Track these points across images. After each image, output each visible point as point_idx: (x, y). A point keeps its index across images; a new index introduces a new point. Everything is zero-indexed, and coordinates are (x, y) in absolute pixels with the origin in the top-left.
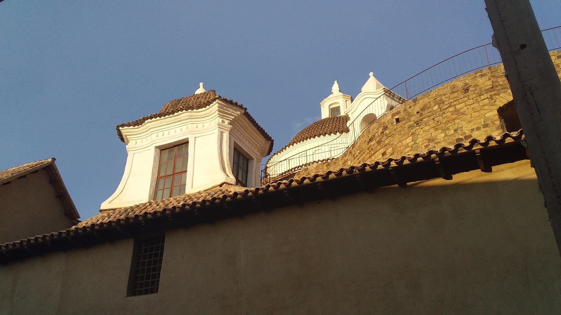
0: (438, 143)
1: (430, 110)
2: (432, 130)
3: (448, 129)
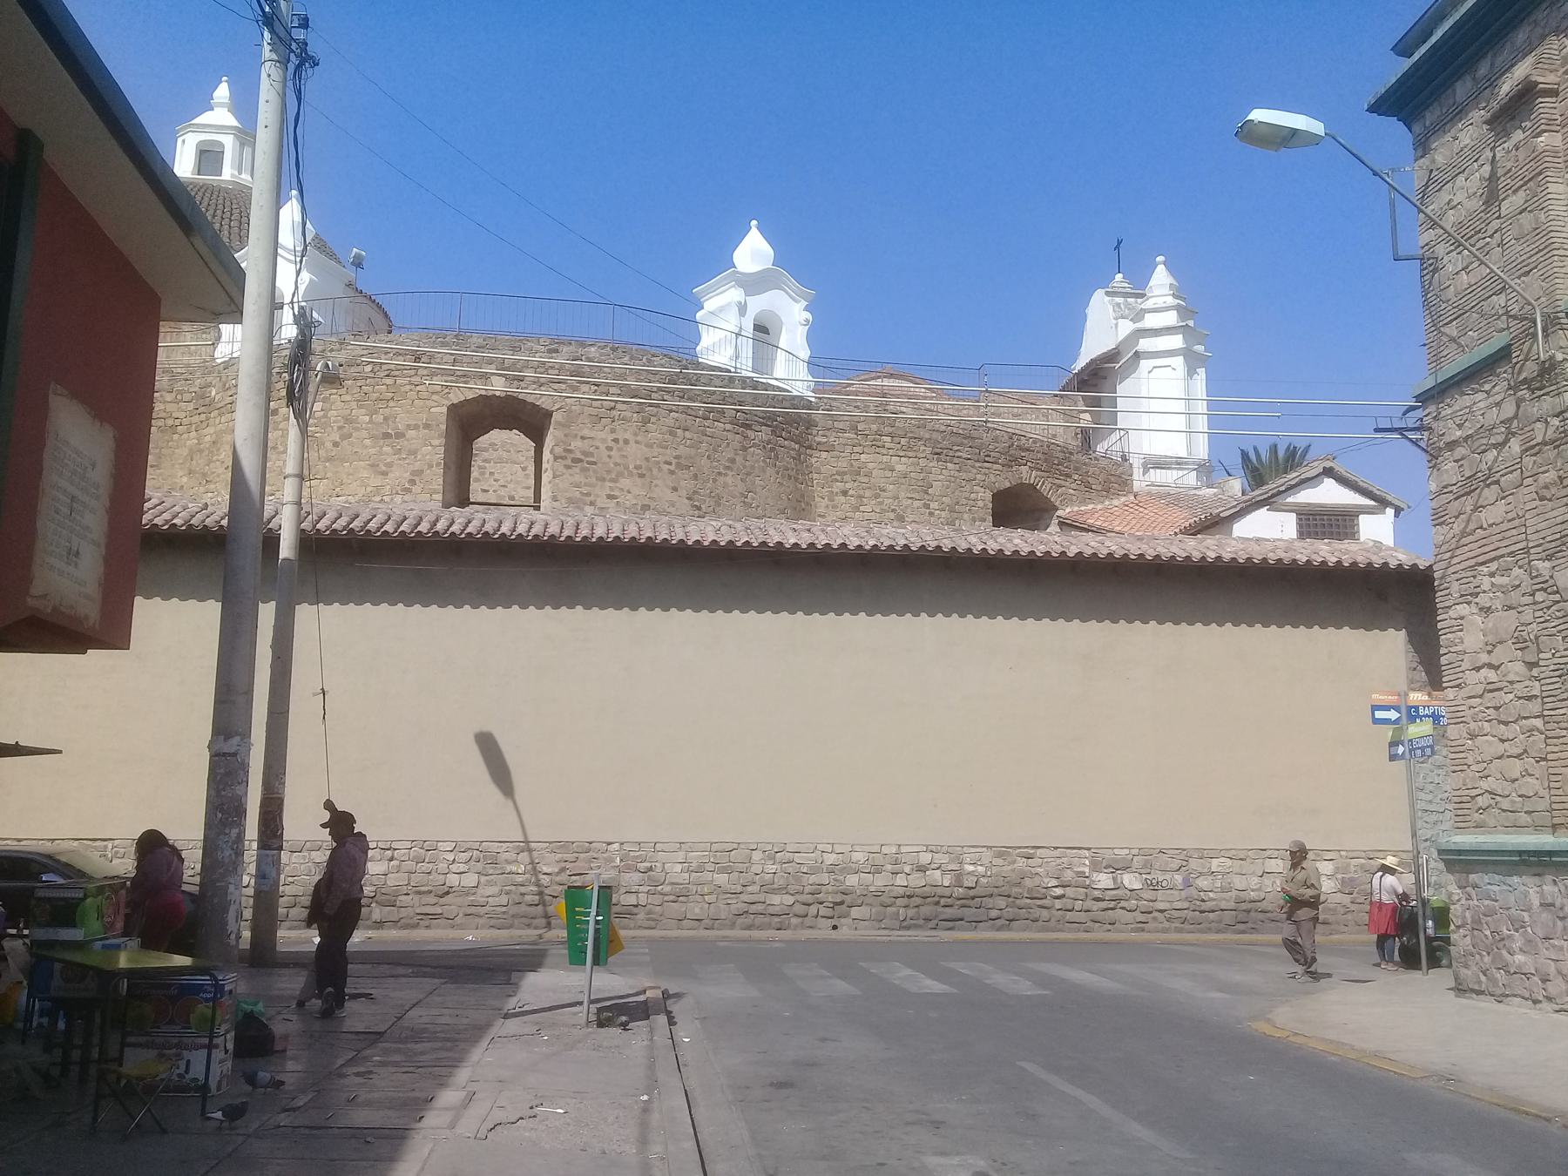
0: (357, 429)
1: (359, 369)
2: (354, 405)
3: (376, 412)
